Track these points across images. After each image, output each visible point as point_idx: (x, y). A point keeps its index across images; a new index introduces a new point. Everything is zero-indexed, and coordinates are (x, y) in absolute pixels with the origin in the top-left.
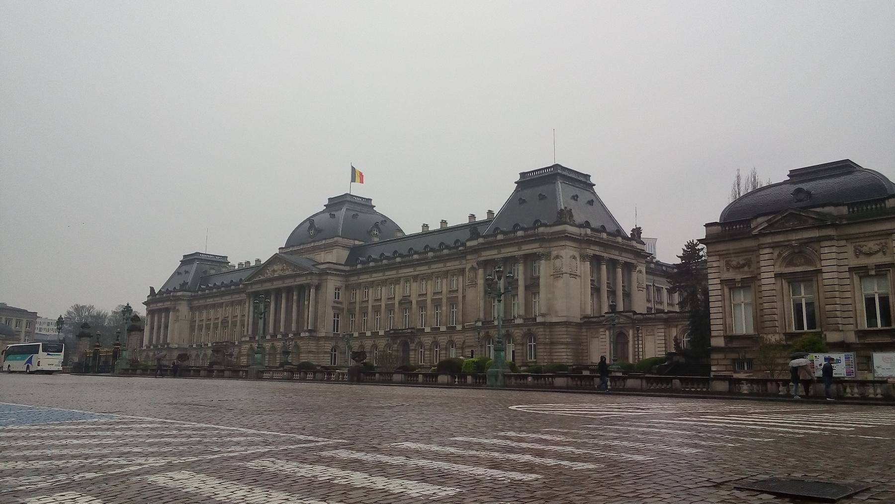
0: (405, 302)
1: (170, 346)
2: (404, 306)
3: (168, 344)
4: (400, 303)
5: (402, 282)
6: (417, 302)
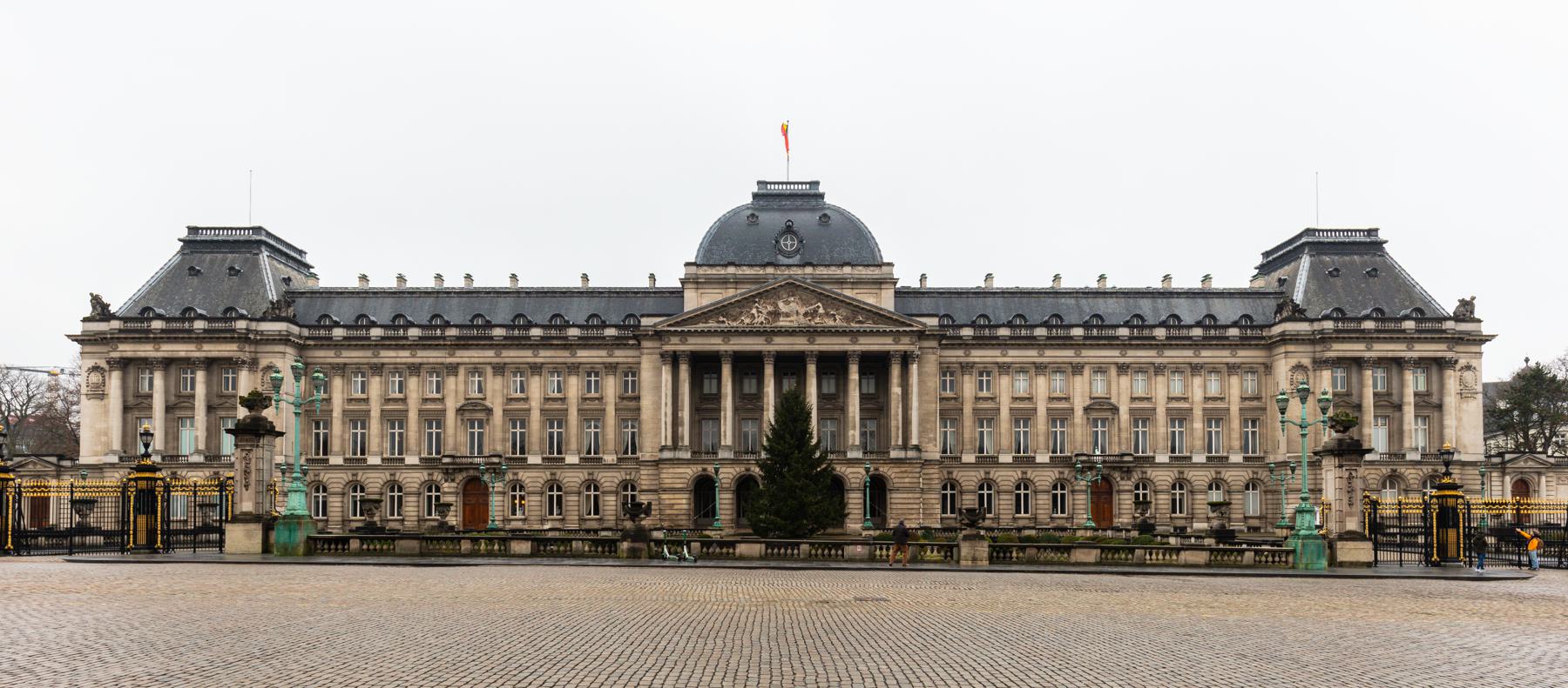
0: (1101, 409)
2: (1094, 415)
4: (1086, 409)
5: (1087, 371)
6: (1131, 410)
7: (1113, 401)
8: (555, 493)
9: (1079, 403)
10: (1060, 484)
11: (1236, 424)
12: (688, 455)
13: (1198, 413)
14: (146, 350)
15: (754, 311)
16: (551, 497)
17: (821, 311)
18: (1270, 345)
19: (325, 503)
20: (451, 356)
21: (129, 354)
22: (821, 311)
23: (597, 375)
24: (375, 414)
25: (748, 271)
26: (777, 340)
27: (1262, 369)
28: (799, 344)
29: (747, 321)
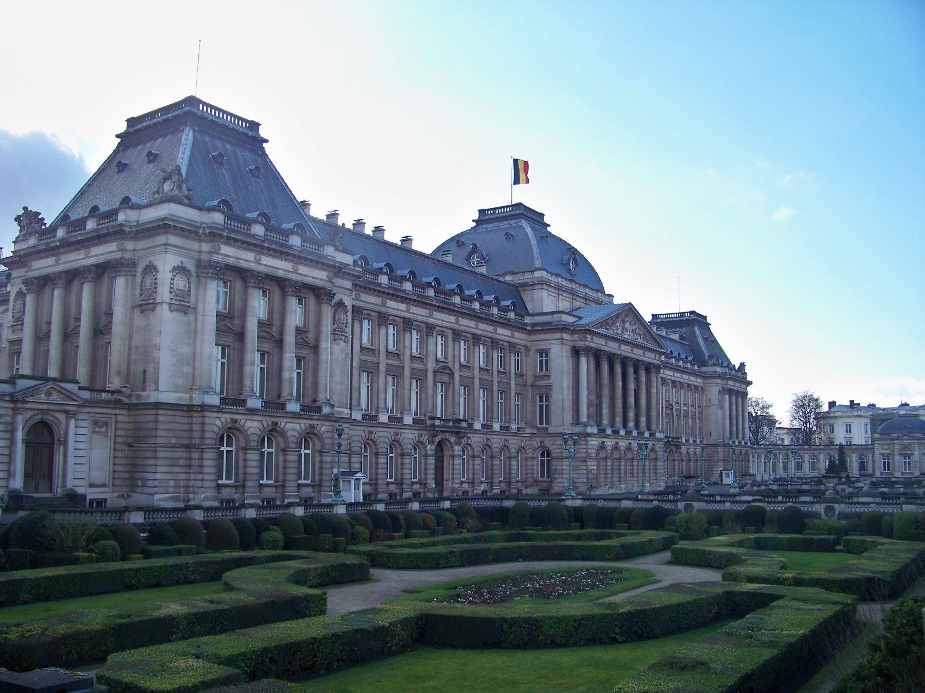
14: (246, 258)
20: (431, 316)
21: (231, 261)
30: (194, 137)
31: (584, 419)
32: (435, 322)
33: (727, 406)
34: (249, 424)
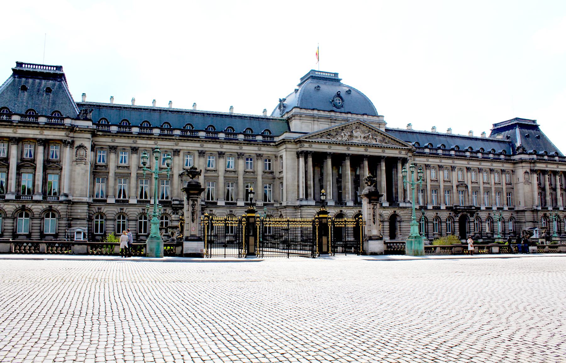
0: (462, 185)
1: (70, 198)
2: (460, 189)
3: (66, 195)
4: (457, 186)
5: (456, 170)
7: (466, 183)
8: (143, 220)
9: (455, 183)
10: (450, 218)
11: (505, 194)
12: (313, 203)
13: (493, 189)
15: (343, 134)
16: (141, 223)
17: (371, 137)
18: (515, 163)
19: (102, 225)
20: (177, 145)
22: (371, 137)
23: (251, 160)
24: (134, 175)
25: (322, 113)
26: (352, 148)
27: (511, 172)
28: (361, 151)
29: (340, 139)
30: (14, 81)
31: (301, 197)
32: (181, 148)
33: (535, 182)
34: (6, 206)
